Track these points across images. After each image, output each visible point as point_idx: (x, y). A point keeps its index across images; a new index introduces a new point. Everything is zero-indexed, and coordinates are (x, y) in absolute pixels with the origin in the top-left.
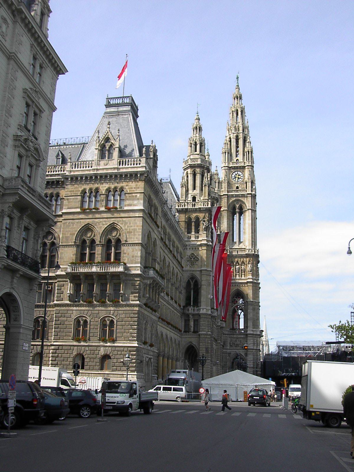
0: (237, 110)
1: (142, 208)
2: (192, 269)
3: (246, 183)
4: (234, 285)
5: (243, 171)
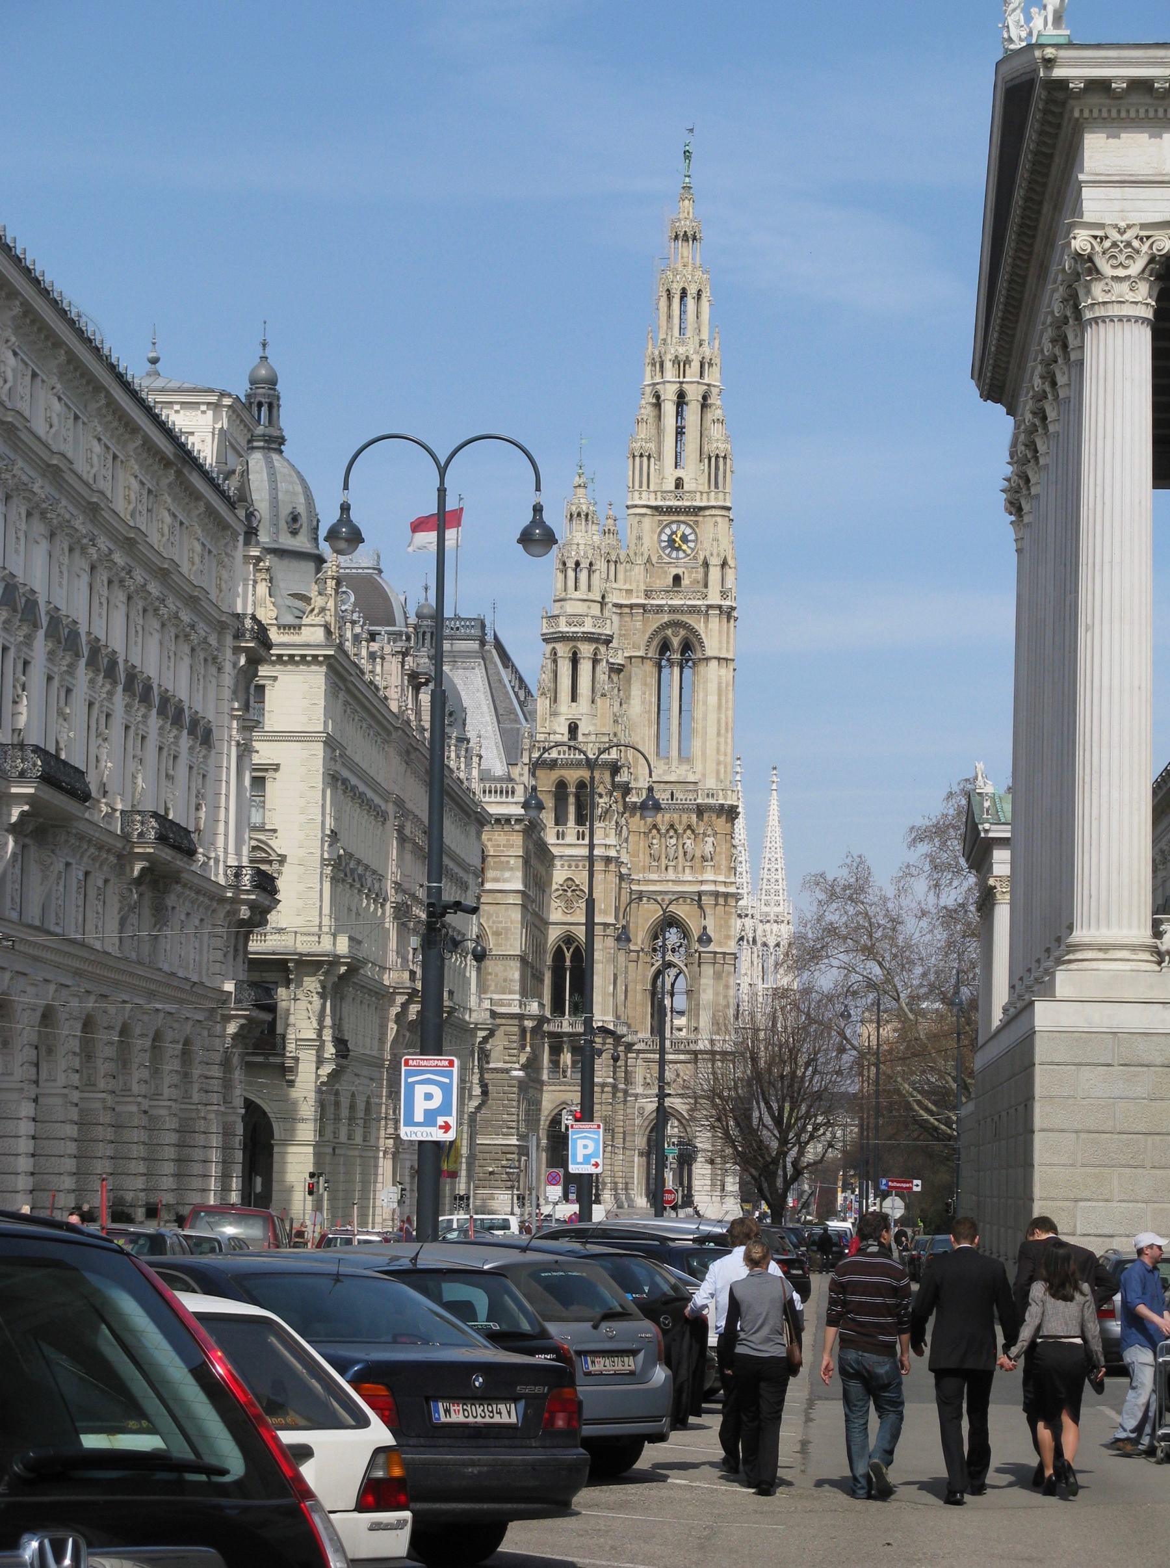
1: (520, 887)
2: (569, 919)
3: (706, 564)
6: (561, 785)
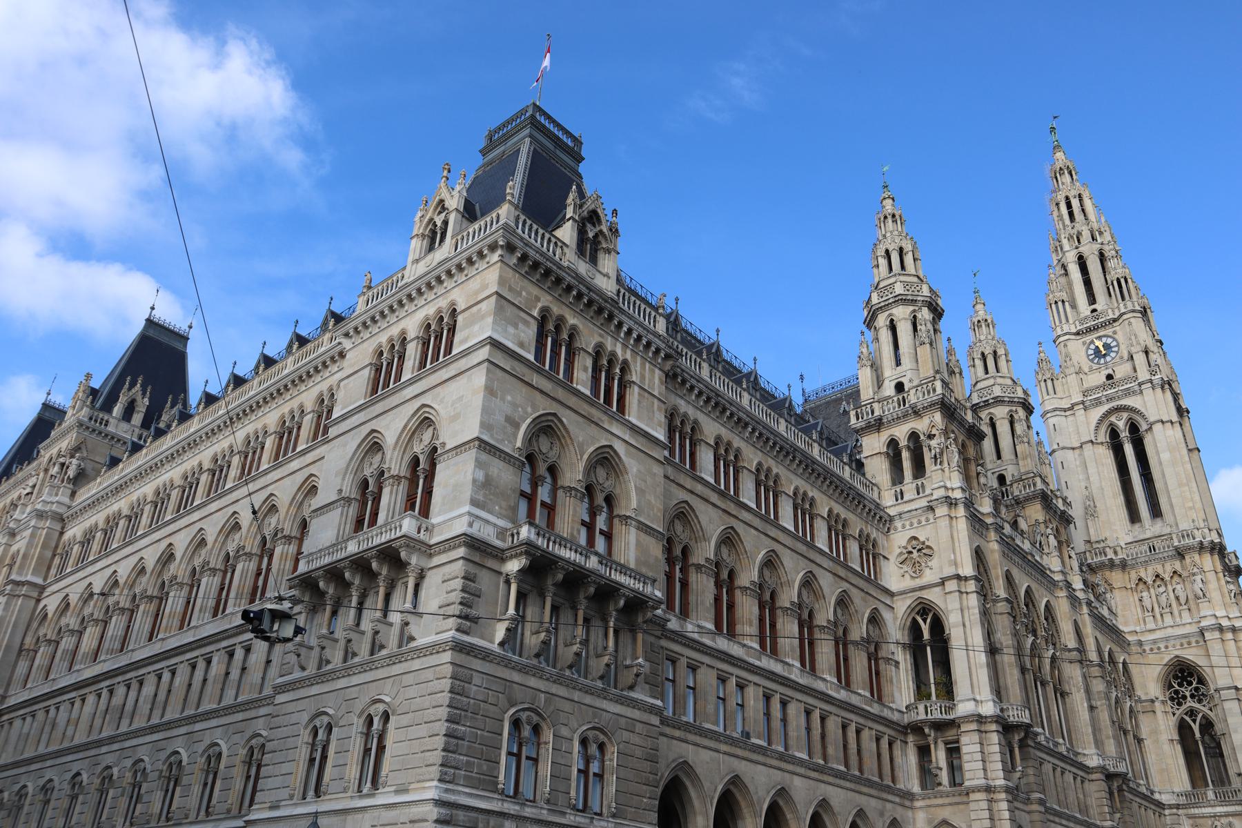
0: (1067, 198)
4: (1162, 646)
5: (1115, 333)
6: (893, 443)
